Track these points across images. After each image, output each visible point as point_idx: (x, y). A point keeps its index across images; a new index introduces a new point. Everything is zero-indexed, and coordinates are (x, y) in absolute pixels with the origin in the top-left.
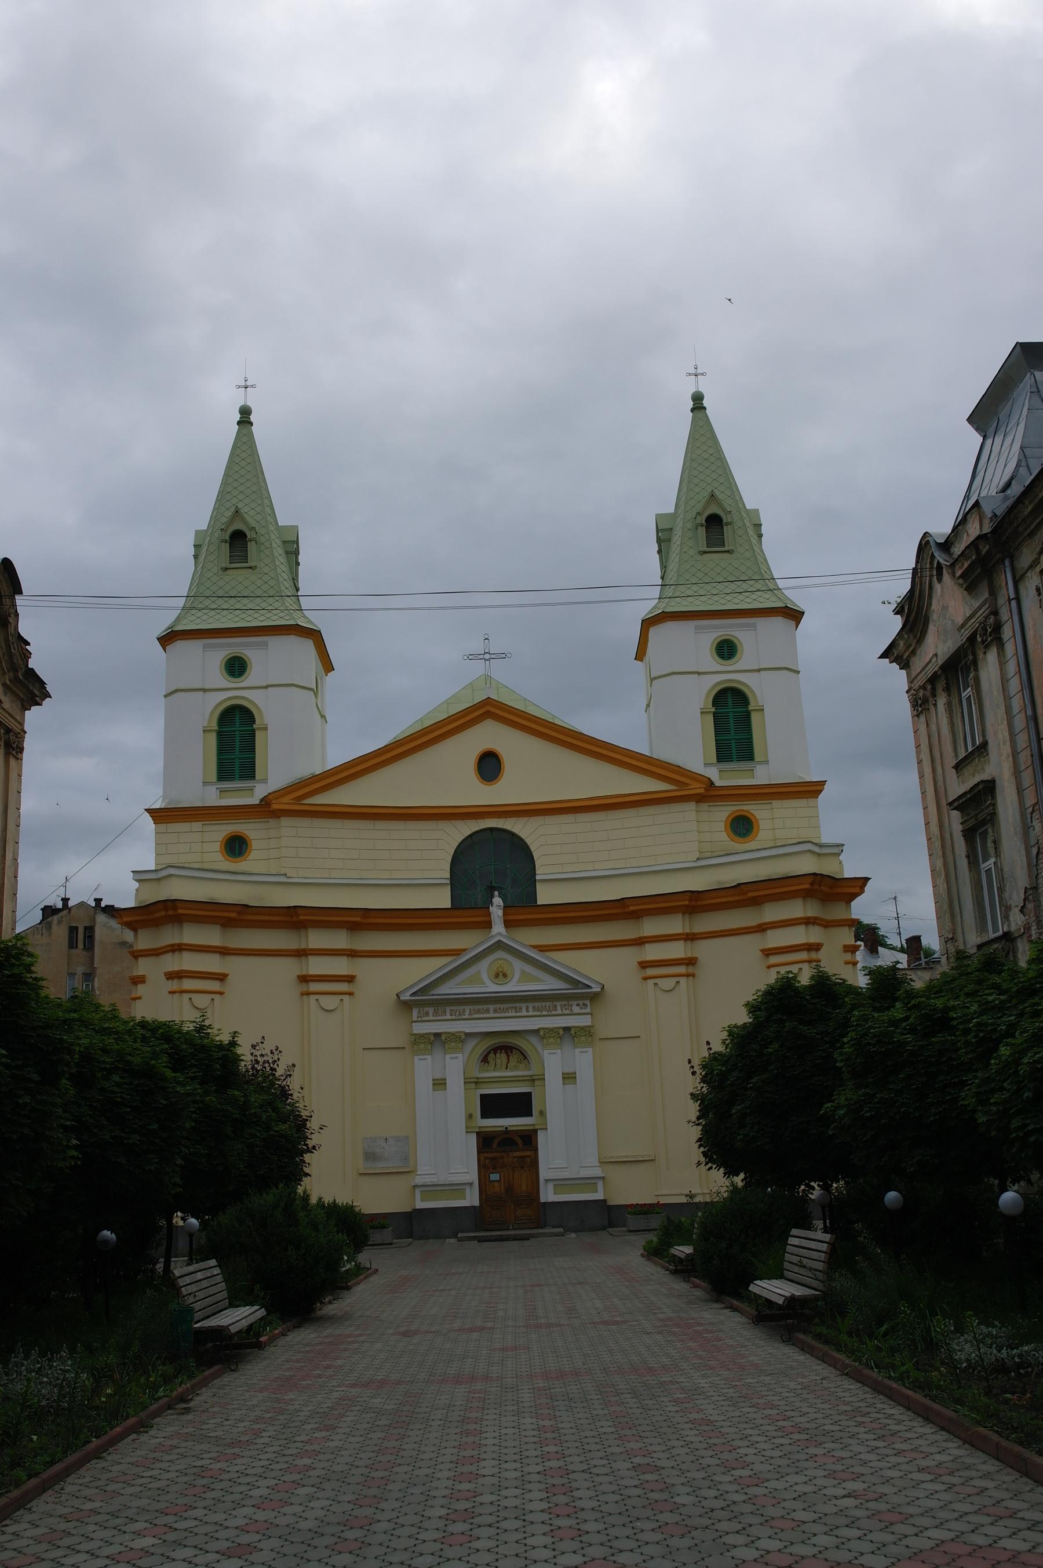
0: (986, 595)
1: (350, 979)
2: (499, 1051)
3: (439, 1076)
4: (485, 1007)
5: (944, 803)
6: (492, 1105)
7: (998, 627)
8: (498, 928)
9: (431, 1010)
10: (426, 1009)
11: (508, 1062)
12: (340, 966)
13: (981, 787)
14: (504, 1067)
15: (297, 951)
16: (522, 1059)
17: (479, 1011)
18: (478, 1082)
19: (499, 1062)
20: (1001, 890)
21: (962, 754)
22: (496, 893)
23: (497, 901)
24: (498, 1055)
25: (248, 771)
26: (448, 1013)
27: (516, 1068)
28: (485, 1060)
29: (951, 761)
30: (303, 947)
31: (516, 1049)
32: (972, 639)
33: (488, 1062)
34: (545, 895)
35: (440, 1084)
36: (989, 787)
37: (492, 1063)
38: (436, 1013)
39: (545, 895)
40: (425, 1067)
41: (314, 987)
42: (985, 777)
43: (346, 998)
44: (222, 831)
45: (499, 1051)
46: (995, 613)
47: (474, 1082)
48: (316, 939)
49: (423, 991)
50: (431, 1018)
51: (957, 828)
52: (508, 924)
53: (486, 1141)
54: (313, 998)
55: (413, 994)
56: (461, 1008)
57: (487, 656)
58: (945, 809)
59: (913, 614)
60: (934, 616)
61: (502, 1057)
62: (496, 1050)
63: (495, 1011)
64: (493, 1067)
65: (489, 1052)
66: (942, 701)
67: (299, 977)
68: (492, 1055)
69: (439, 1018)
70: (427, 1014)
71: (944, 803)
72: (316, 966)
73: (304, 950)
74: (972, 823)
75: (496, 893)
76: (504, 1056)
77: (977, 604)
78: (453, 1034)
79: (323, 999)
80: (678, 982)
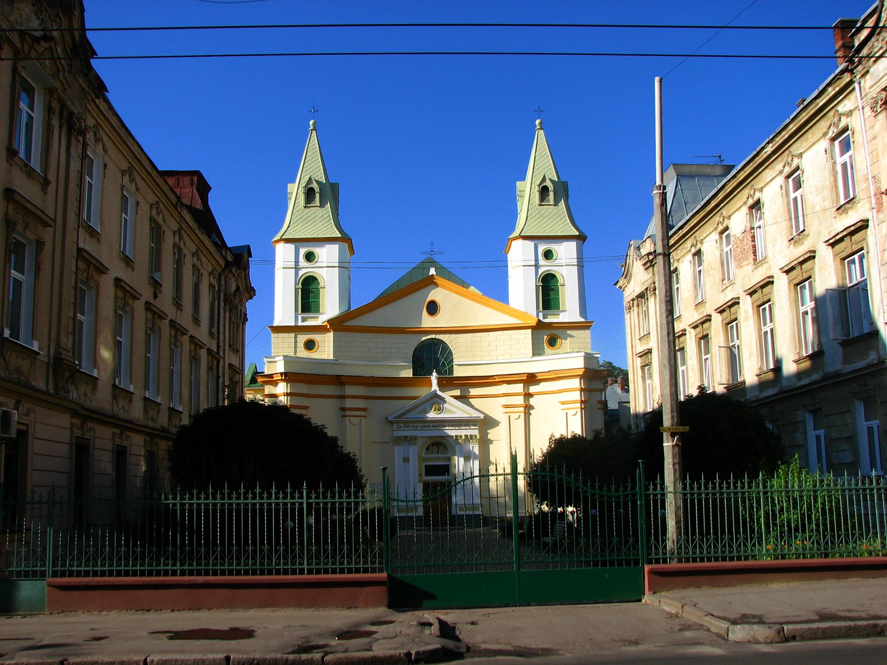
0: (652, 275)
1: (364, 410)
3: (406, 456)
4: (428, 424)
5: (634, 354)
6: (431, 470)
7: (655, 289)
8: (435, 387)
9: (402, 425)
12: (361, 404)
13: (647, 351)
15: (341, 396)
17: (425, 426)
18: (425, 460)
19: (434, 450)
20: (652, 394)
21: (642, 335)
22: (435, 370)
23: (435, 374)
25: (317, 310)
27: (442, 453)
28: (427, 449)
29: (638, 337)
30: (343, 394)
32: (646, 289)
34: (458, 372)
35: (406, 460)
36: (650, 351)
38: (405, 427)
39: (458, 372)
40: (398, 452)
41: (348, 413)
42: (649, 347)
43: (363, 419)
44: (303, 338)
46: (654, 283)
47: (421, 459)
48: (350, 390)
49: (399, 416)
51: (639, 365)
52: (440, 384)
53: (426, 486)
54: (347, 418)
55: (394, 418)
57: (432, 253)
58: (635, 356)
59: (626, 272)
60: (633, 275)
61: (435, 448)
62: (433, 444)
63: (433, 426)
65: (429, 446)
66: (636, 309)
67: (340, 408)
68: (431, 446)
70: (401, 427)
71: (634, 354)
72: (349, 403)
73: (343, 396)
74: (644, 364)
75: (435, 370)
77: (649, 277)
79: (353, 419)
80: (520, 416)
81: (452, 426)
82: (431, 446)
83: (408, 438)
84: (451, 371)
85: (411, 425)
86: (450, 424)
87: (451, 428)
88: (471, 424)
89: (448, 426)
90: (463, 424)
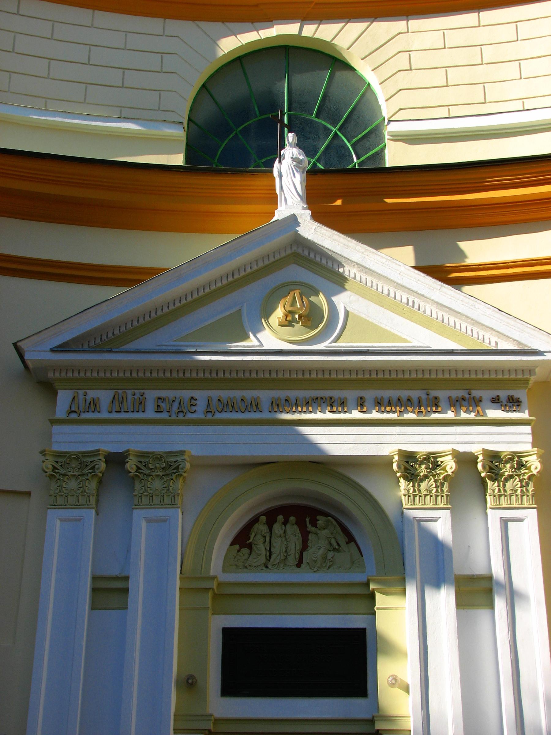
2: (280, 518)
4: (249, 394)
10: (92, 394)
11: (305, 547)
14: (292, 560)
16: (342, 539)
19: (278, 545)
24: (277, 527)
26: (150, 406)
31: (326, 515)
33: (250, 547)
37: (261, 548)
45: (280, 518)
50: (105, 415)
55: (62, 348)
56: (186, 394)
64: (263, 559)
65: (255, 521)
68: (261, 527)
69: (123, 416)
70: (94, 405)
75: (291, 137)
76: (293, 530)
78: (158, 457)
81: (379, 404)
82: (261, 527)
83: (131, 465)
84: (380, 155)
85: (151, 395)
86: (370, 394)
87: (375, 415)
88: (487, 394)
89: (361, 404)
90: (442, 394)
